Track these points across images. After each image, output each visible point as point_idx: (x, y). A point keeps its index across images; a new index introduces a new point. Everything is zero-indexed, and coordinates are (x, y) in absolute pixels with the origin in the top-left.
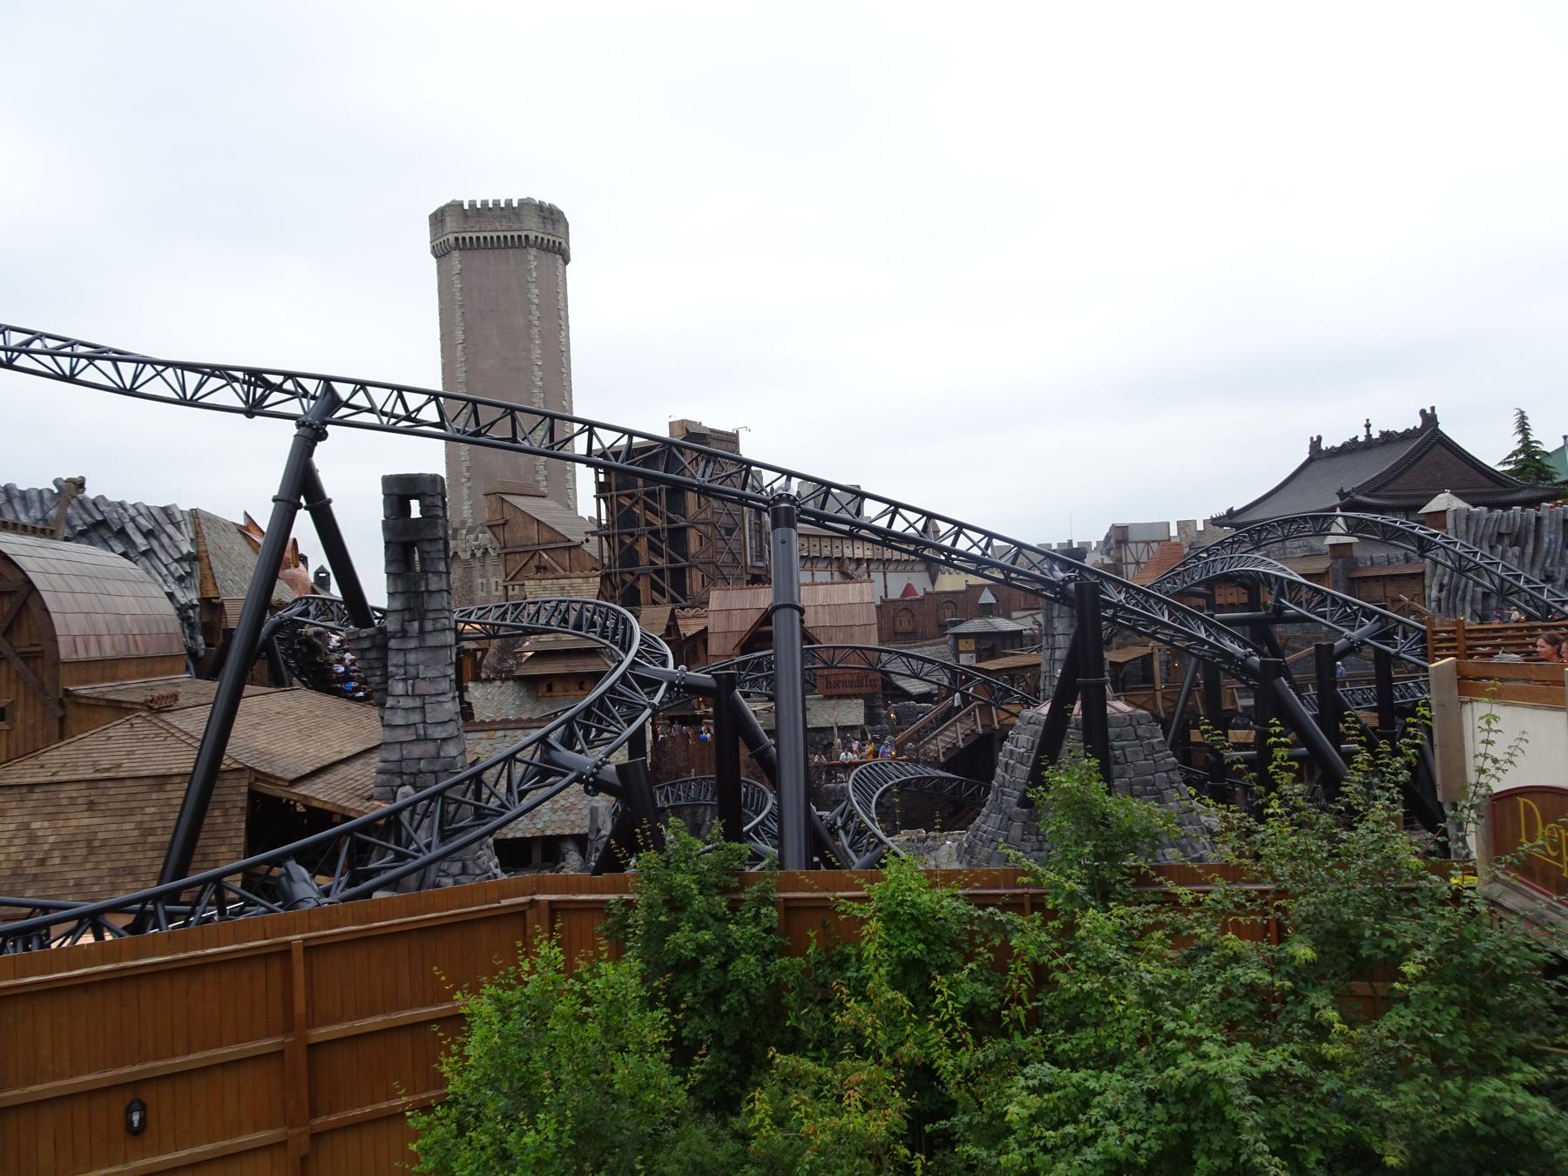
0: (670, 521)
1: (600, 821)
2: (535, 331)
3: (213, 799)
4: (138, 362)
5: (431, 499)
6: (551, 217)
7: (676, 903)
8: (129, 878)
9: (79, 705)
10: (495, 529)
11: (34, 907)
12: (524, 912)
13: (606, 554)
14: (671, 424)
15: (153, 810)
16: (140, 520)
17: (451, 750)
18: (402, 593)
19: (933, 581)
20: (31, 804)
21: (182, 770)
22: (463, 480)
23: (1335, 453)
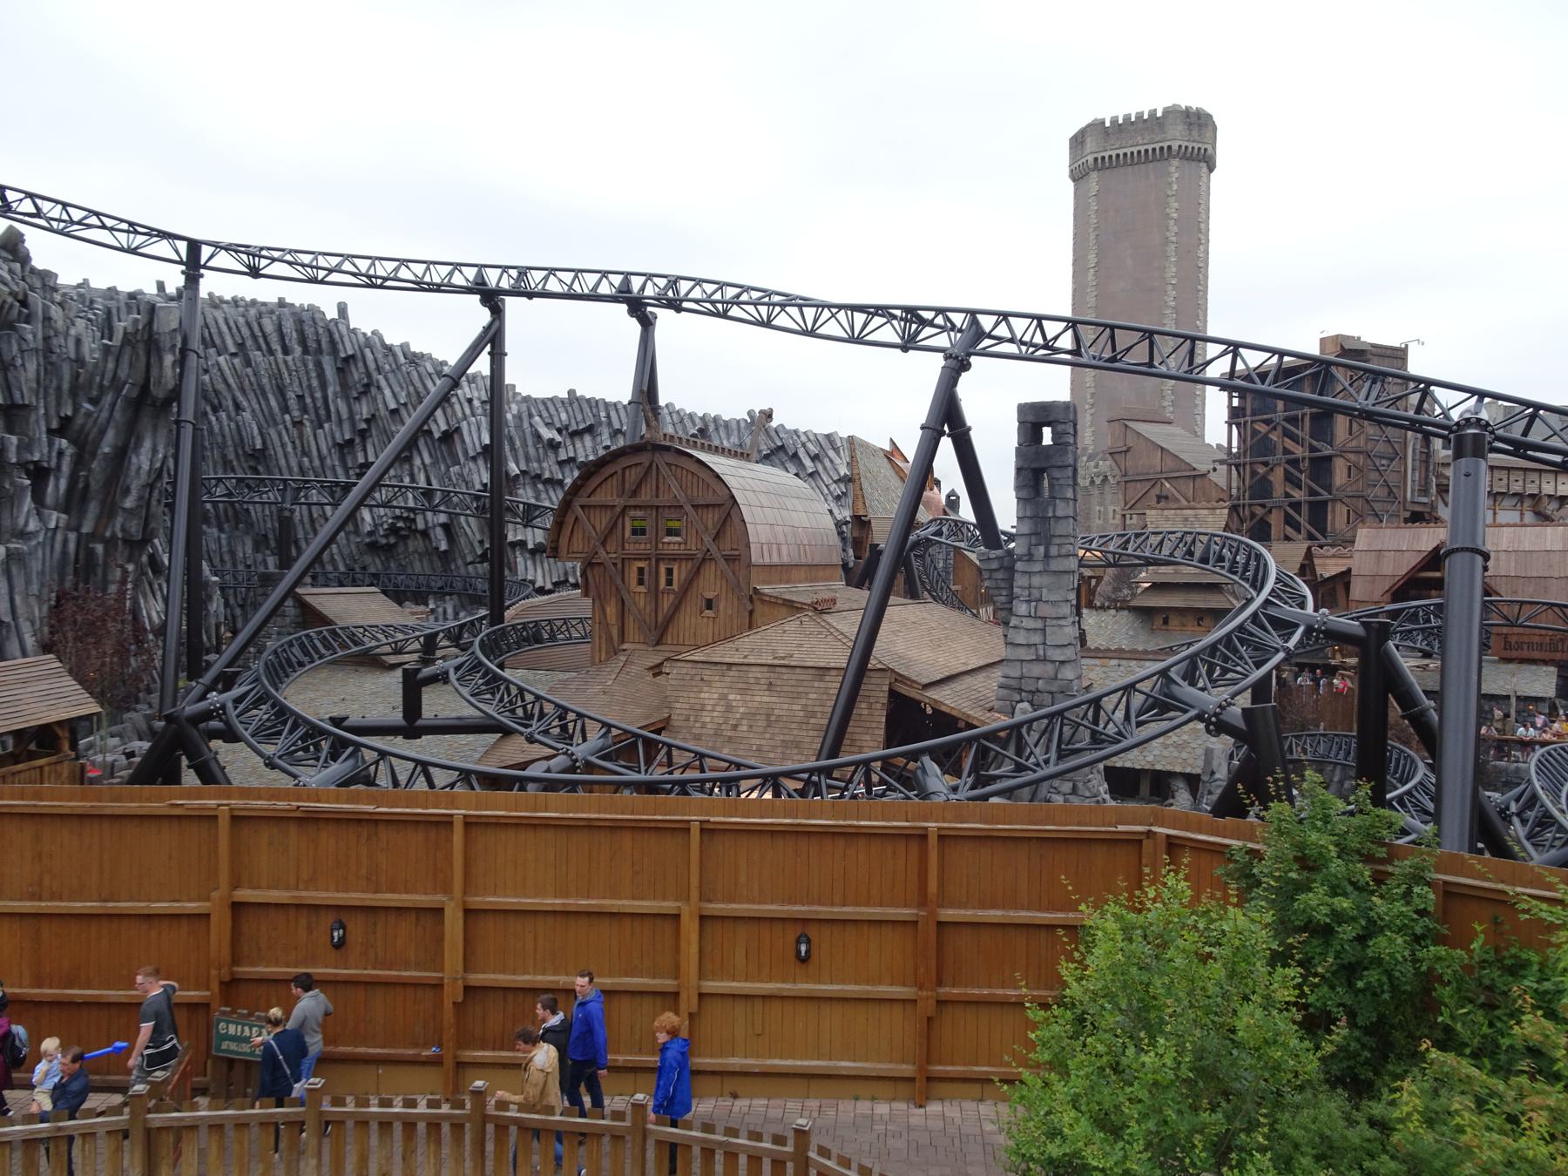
0: (1313, 449)
1: (1215, 763)
3: (861, 693)
4: (817, 306)
5: (1063, 426)
6: (1199, 122)
7: (1308, 862)
8: (796, 751)
9: (763, 602)
10: (1116, 456)
11: (731, 763)
12: (1140, 841)
13: (1234, 484)
14: (1322, 341)
15: (814, 696)
16: (810, 445)
17: (1068, 673)
21: (838, 665)
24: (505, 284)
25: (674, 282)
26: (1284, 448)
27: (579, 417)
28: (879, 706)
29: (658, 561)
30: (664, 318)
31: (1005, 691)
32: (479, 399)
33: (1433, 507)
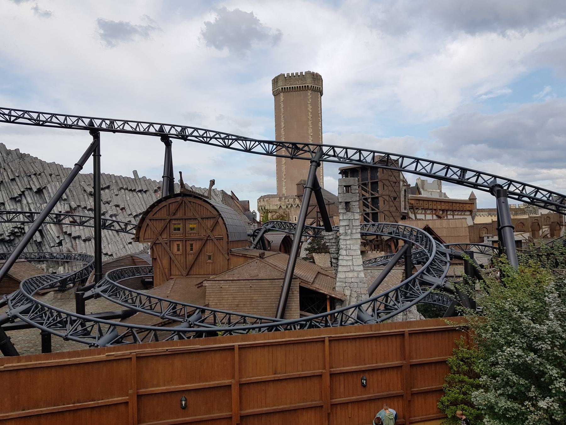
0: (372, 194)
6: (317, 78)
10: (300, 197)
19: (473, 219)
24: (104, 126)
25: (184, 128)
26: (362, 194)
30: (176, 144)
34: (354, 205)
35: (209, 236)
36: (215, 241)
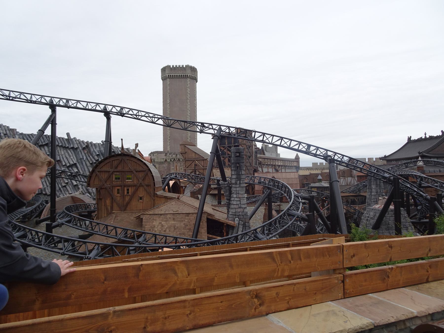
2: (189, 100)
6: (194, 70)
9: (157, 197)
15: (187, 221)
18: (236, 174)
20: (162, 218)
22: (168, 140)
23: (415, 141)
25: (122, 108)
27: (43, 141)
28: (205, 222)
29: (124, 187)
31: (232, 216)
32: (3, 133)
33: (257, 168)
34: (242, 165)
35: (141, 183)
36: (145, 187)
